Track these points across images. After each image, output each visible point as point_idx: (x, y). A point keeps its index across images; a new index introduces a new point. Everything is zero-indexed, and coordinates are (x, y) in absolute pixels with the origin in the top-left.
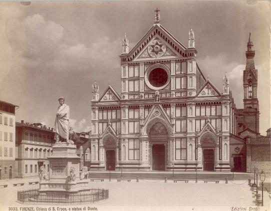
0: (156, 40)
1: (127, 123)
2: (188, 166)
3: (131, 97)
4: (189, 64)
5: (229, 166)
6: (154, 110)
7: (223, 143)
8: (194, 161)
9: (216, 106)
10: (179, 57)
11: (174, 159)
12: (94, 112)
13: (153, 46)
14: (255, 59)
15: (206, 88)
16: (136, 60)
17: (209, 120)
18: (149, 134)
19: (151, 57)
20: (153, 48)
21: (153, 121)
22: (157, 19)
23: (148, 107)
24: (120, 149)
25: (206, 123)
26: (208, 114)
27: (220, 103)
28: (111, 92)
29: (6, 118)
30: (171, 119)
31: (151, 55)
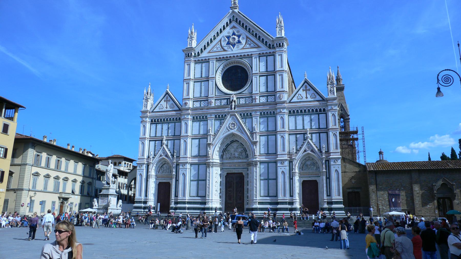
0: (234, 29)
2: (279, 206)
3: (197, 105)
4: (278, 58)
5: (342, 206)
6: (229, 120)
9: (319, 114)
10: (264, 49)
11: (258, 195)
12: (144, 127)
13: (228, 37)
14: (345, 92)
15: (303, 90)
17: (309, 135)
18: (222, 157)
19: (225, 50)
20: (228, 39)
21: (226, 138)
22: (235, 3)
23: (221, 118)
24: (177, 181)
25: (305, 140)
26: (307, 127)
27: (324, 110)
28: (169, 98)
30: (252, 133)
31: (226, 48)
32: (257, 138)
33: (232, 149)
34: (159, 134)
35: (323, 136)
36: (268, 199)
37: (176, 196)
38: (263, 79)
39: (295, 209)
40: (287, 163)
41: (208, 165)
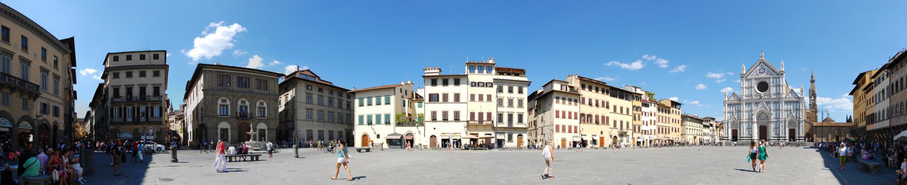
1: (744, 113)
3: (747, 98)
4: (781, 80)
7: (801, 125)
8: (783, 135)
10: (775, 76)
12: (725, 107)
16: (749, 77)
18: (758, 119)
23: (757, 104)
24: (740, 129)
29: (673, 110)
30: (770, 110)
32: (772, 112)
33: (762, 116)
34: (731, 110)
35: (798, 112)
36: (776, 136)
37: (740, 135)
38: (775, 88)
39: (786, 140)
40: (783, 122)
41: (753, 123)
